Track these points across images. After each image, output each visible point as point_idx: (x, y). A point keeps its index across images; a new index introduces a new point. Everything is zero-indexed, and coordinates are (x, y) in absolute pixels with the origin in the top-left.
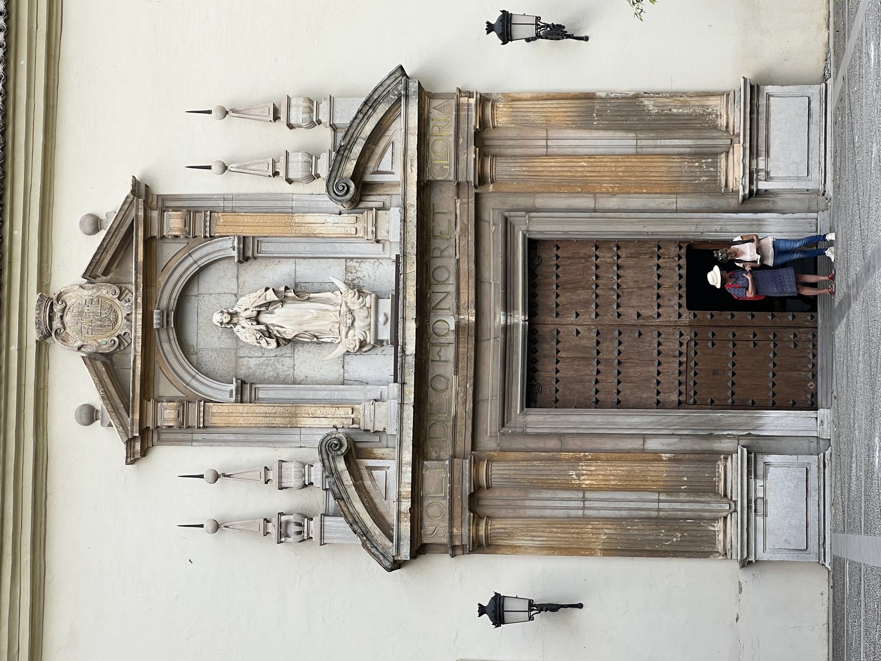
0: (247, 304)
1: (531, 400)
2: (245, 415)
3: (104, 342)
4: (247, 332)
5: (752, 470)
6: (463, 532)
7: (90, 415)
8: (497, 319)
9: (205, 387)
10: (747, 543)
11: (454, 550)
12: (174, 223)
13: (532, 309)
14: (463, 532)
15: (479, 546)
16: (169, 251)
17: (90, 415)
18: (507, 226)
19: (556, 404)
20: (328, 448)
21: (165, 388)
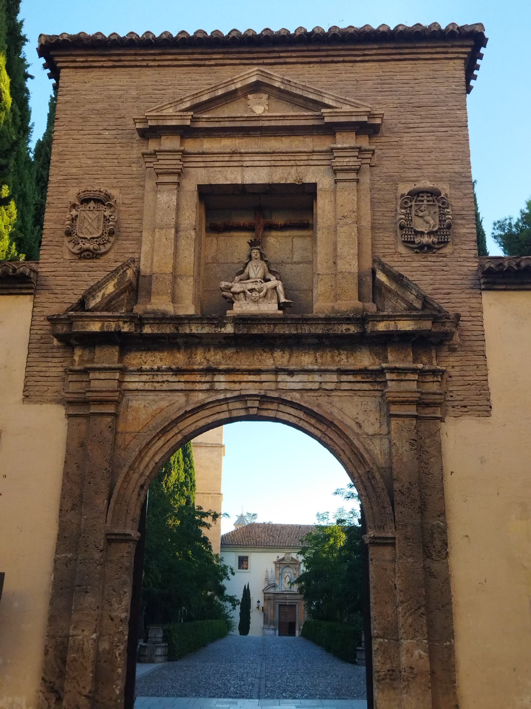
0: (289, 574)
1: (279, 605)
2: (278, 574)
3: (285, 559)
4: (286, 574)
5: (273, 629)
6: (266, 598)
7: (278, 557)
8: (288, 601)
9: (281, 569)
10: (265, 628)
11: (264, 597)
12: (298, 566)
13: (289, 605)
14: (266, 598)
15: (265, 599)
16: (295, 566)
17: (278, 557)
18: (297, 603)
19: (279, 608)
20: (275, 584)
21: (281, 565)
